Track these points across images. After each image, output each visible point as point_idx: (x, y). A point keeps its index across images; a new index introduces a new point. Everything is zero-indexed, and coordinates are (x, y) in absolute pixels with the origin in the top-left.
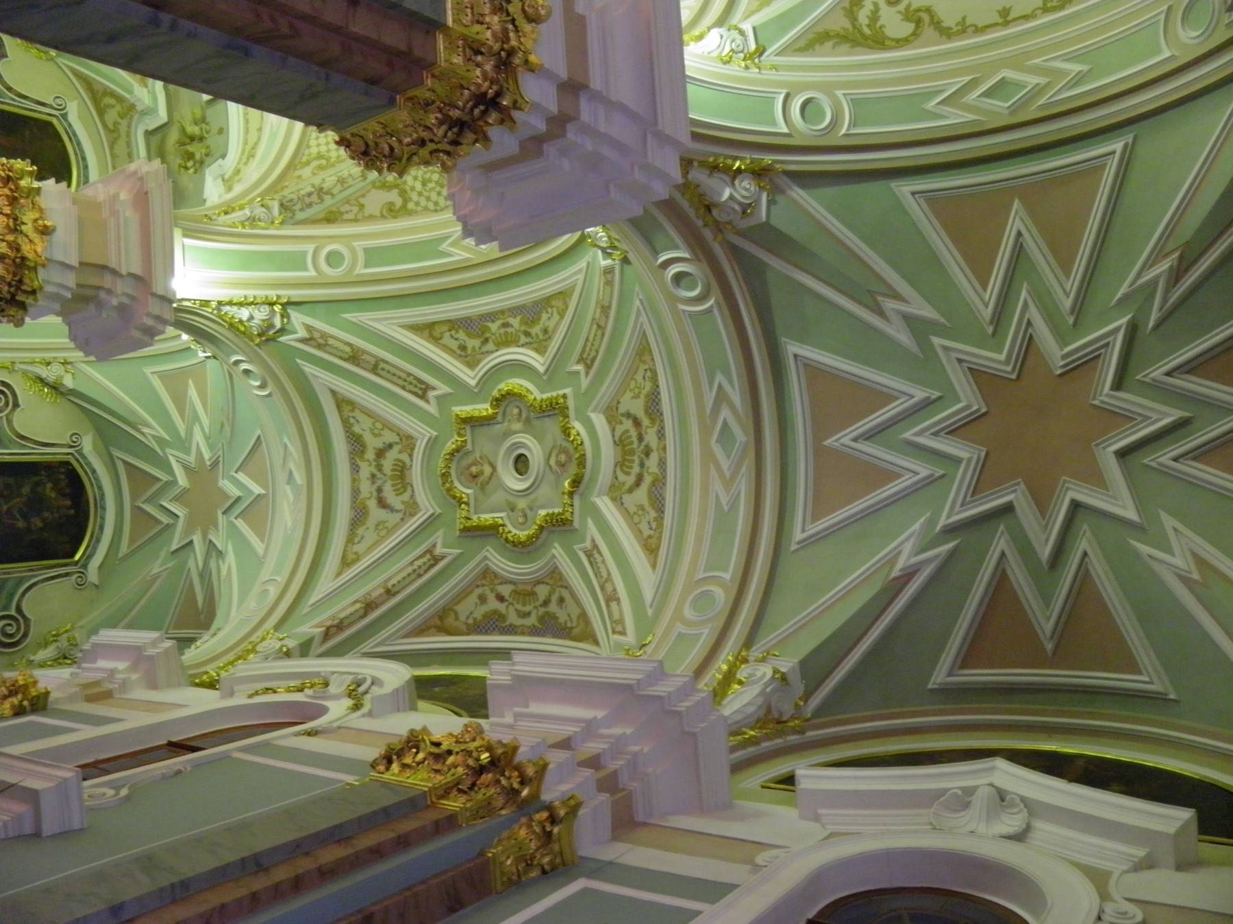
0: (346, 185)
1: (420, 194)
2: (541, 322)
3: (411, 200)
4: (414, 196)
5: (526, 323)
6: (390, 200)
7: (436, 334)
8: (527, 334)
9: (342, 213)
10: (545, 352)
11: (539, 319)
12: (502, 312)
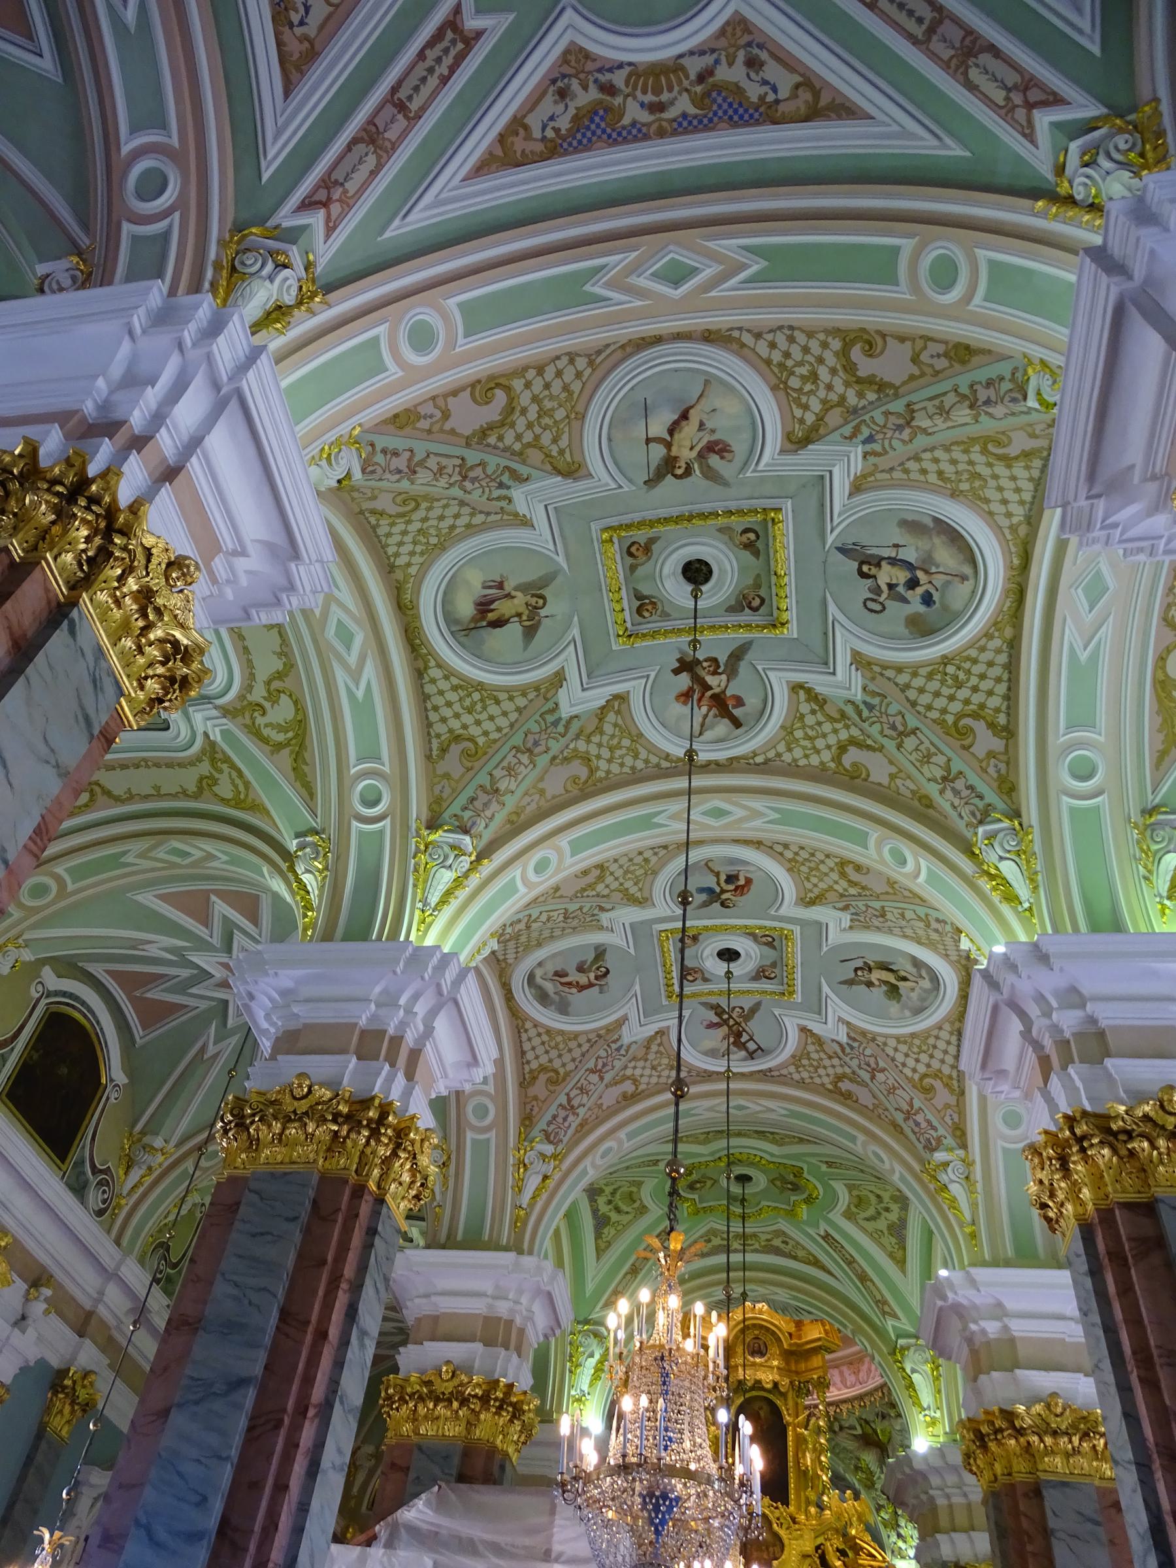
0: (937, 402)
1: (821, 360)
2: (572, 111)
3: (836, 354)
4: (831, 360)
5: (607, 110)
6: (869, 359)
7: (805, 96)
8: (609, 89)
9: (946, 355)
10: (567, 52)
11: (576, 119)
12: (661, 134)
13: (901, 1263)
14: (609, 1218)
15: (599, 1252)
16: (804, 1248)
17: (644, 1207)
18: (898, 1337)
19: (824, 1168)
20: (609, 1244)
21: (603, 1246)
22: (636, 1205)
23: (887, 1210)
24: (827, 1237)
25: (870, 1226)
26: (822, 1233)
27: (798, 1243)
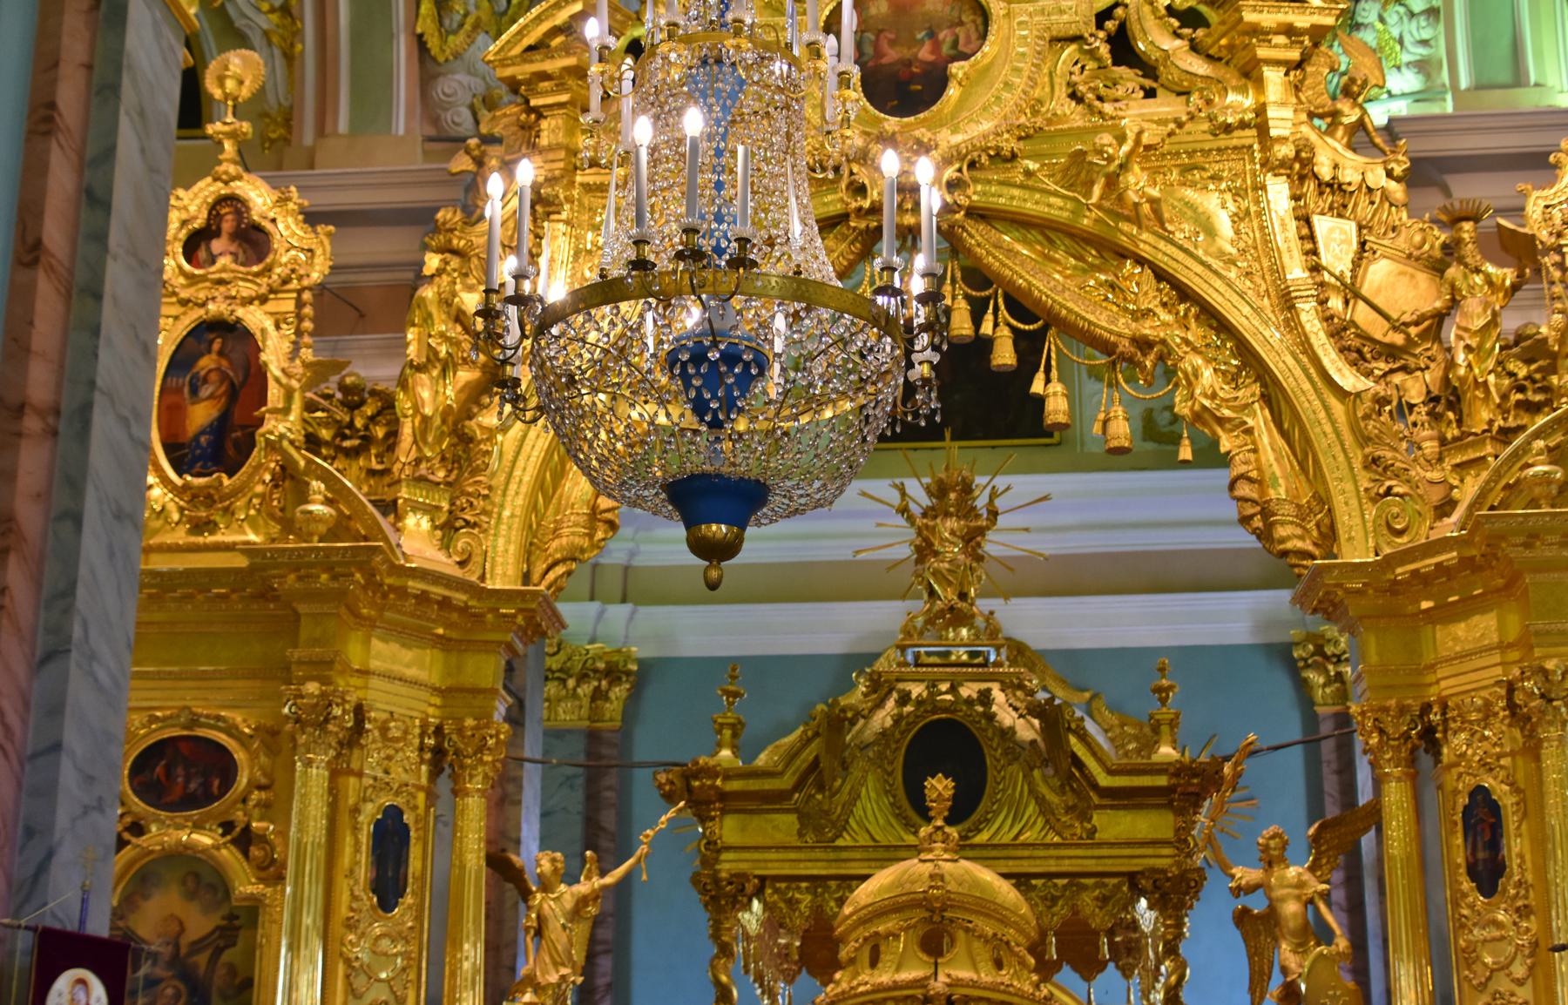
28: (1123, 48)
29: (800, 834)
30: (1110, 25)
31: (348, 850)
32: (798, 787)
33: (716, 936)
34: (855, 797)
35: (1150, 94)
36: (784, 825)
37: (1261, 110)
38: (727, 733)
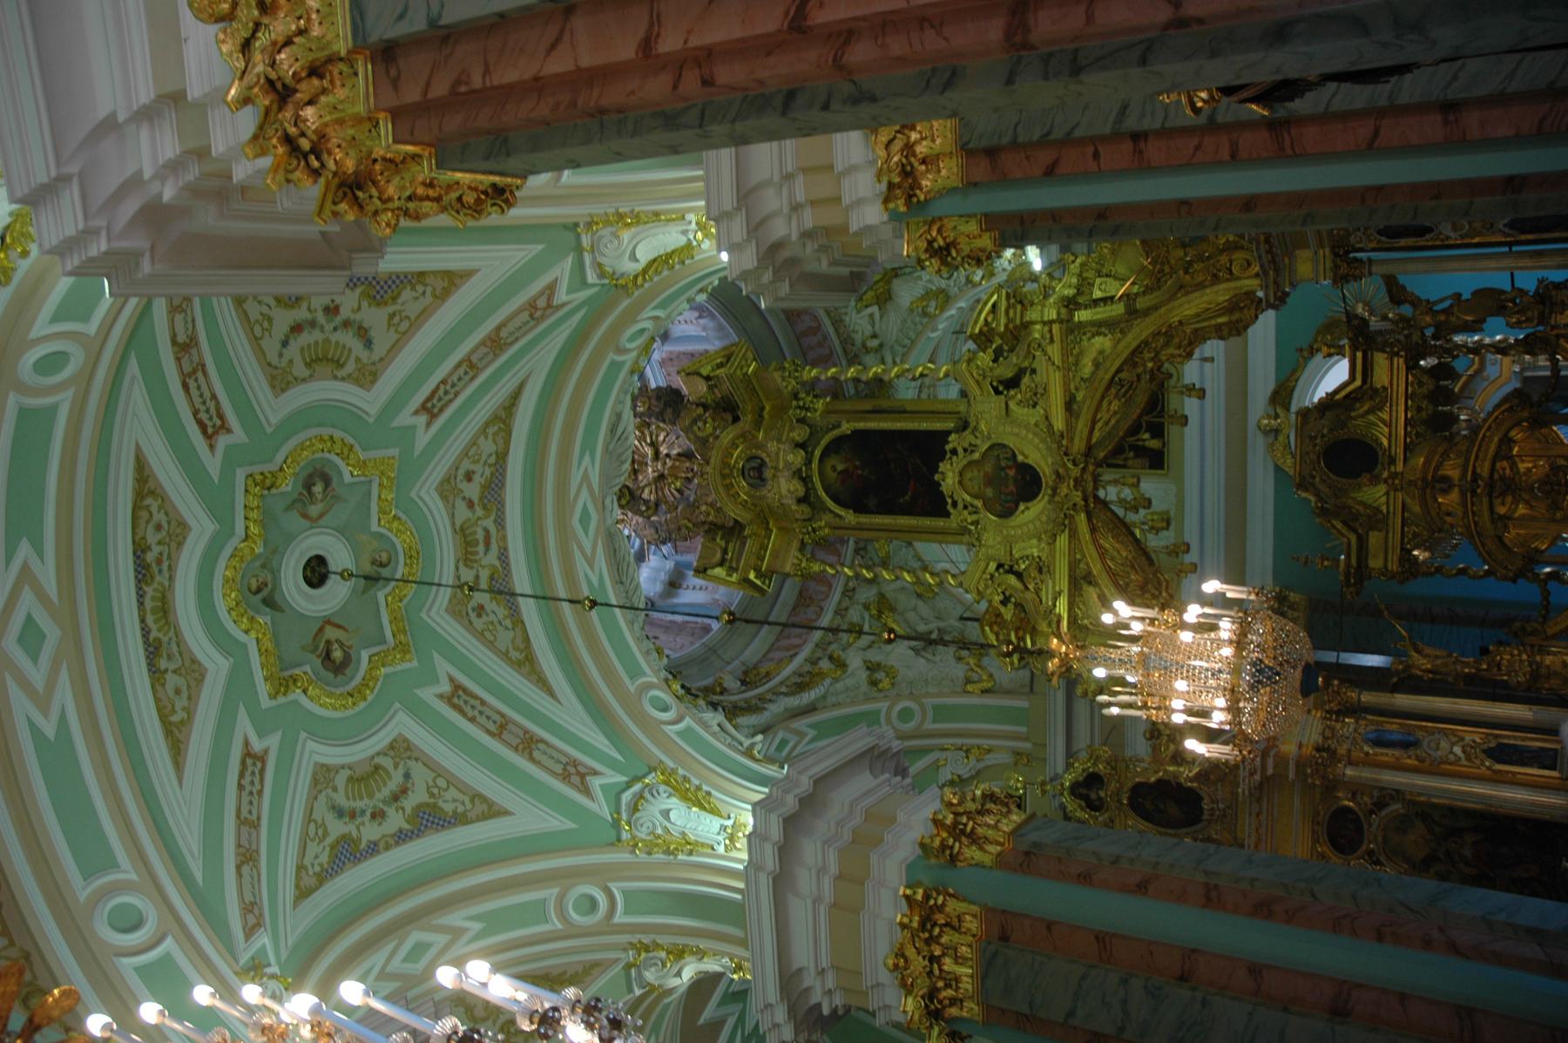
13: (452, 280)
14: (420, 806)
15: (493, 811)
16: (474, 443)
17: (391, 747)
18: (584, 284)
19: (222, 441)
20: (477, 797)
21: (480, 808)
22: (387, 762)
23: (332, 310)
24: (430, 409)
25: (383, 339)
26: (422, 419)
27: (465, 453)
28: (1013, 383)
29: (1380, 530)
30: (1001, 388)
31: (1386, 759)
32: (1354, 530)
33: (1431, 574)
34: (1364, 505)
35: (1034, 371)
36: (1374, 538)
37: (1044, 323)
38: (1326, 563)
